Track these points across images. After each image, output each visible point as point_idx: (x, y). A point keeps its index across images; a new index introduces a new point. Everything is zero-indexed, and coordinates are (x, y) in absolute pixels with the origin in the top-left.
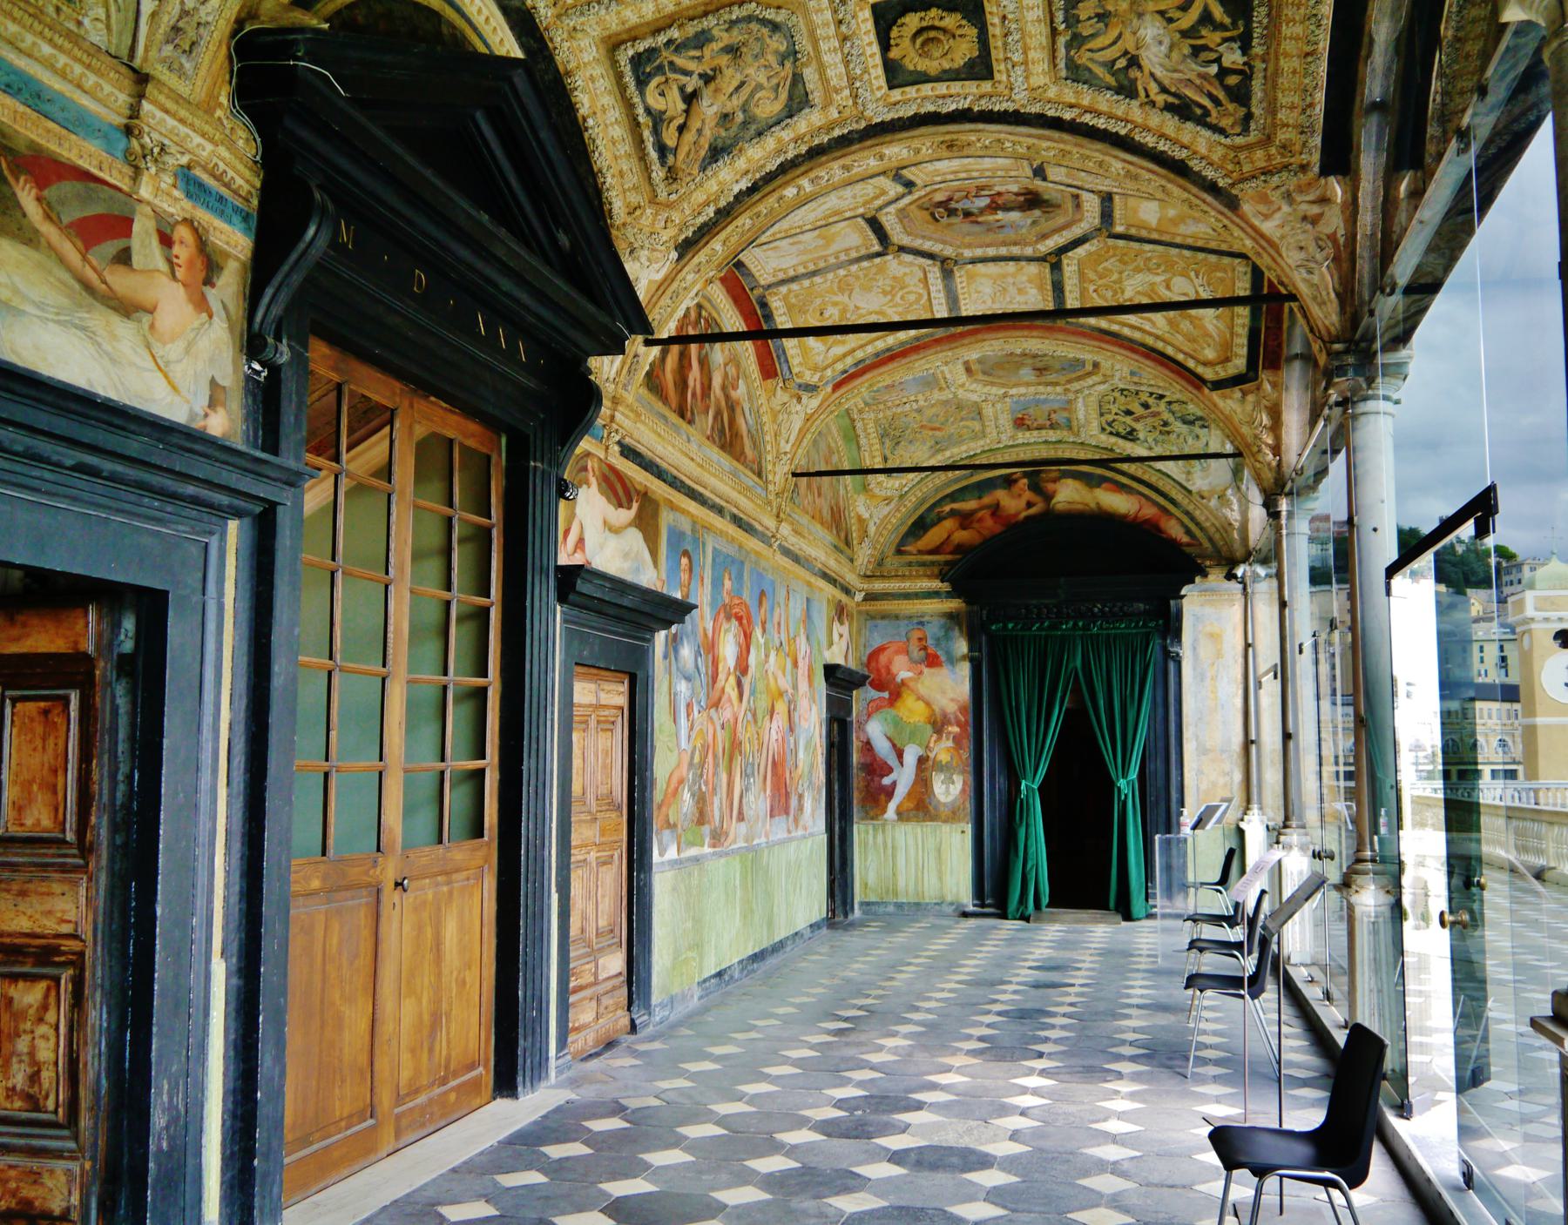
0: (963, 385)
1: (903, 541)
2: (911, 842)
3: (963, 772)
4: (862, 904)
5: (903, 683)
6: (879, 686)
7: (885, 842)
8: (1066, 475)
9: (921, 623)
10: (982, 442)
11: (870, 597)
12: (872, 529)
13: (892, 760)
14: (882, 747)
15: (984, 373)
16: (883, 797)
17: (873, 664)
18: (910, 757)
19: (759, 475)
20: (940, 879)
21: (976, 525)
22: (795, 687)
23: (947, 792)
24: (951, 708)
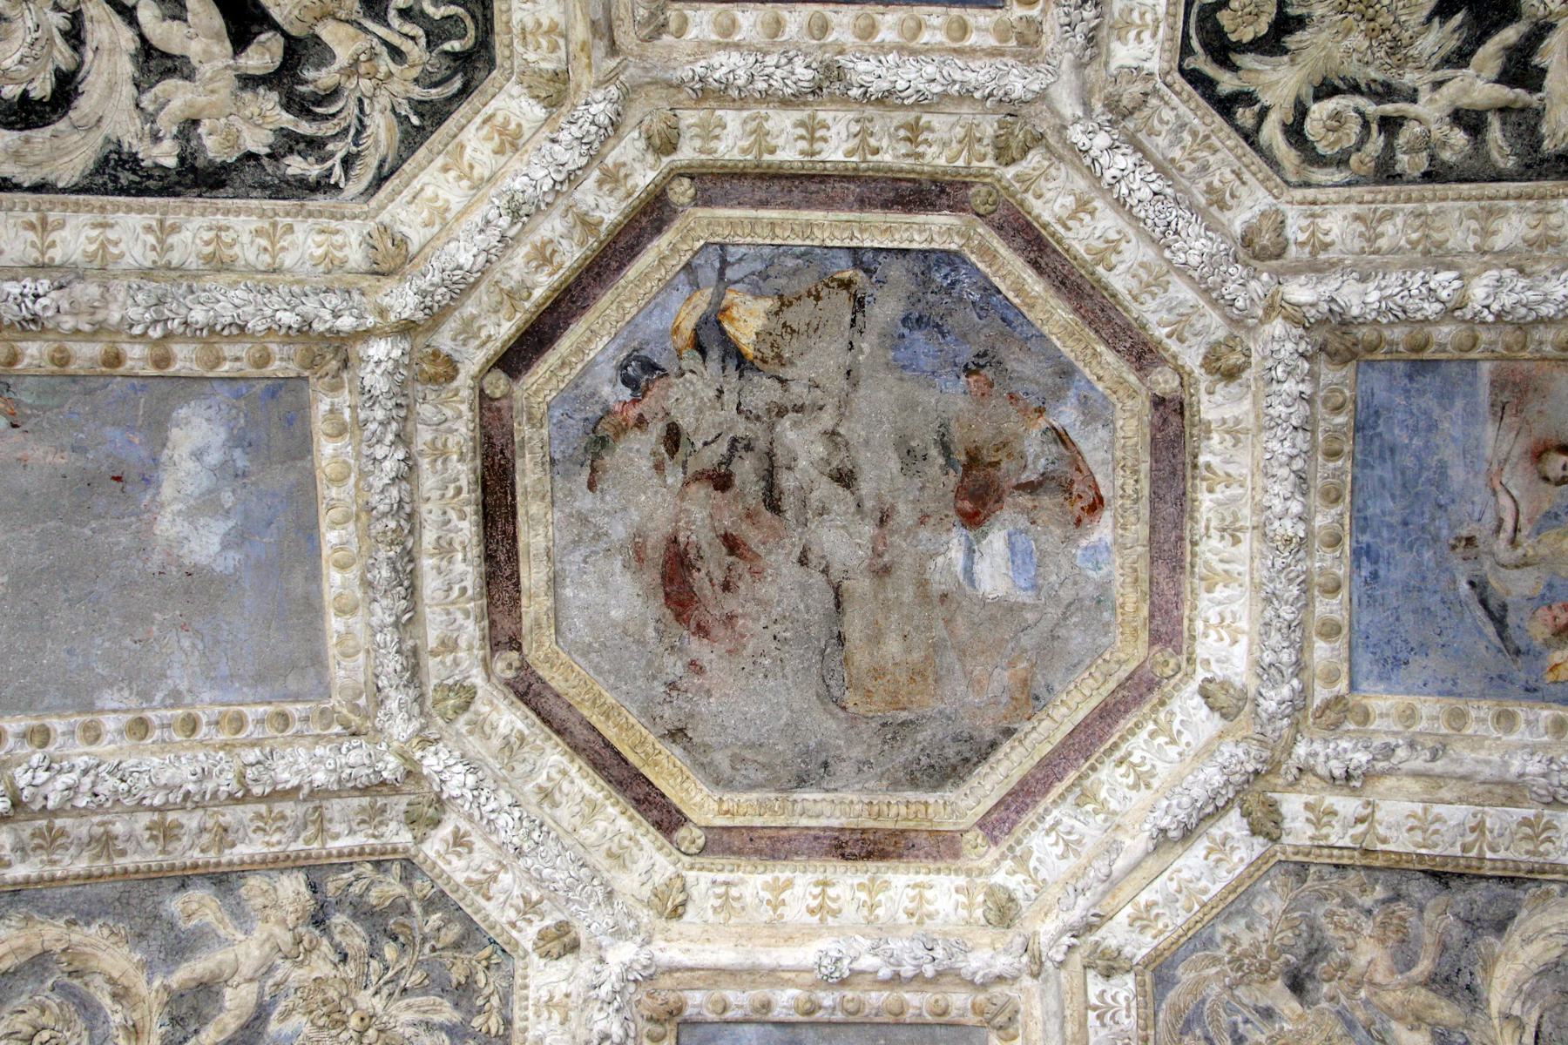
0: (1004, 912)
15: (946, 772)
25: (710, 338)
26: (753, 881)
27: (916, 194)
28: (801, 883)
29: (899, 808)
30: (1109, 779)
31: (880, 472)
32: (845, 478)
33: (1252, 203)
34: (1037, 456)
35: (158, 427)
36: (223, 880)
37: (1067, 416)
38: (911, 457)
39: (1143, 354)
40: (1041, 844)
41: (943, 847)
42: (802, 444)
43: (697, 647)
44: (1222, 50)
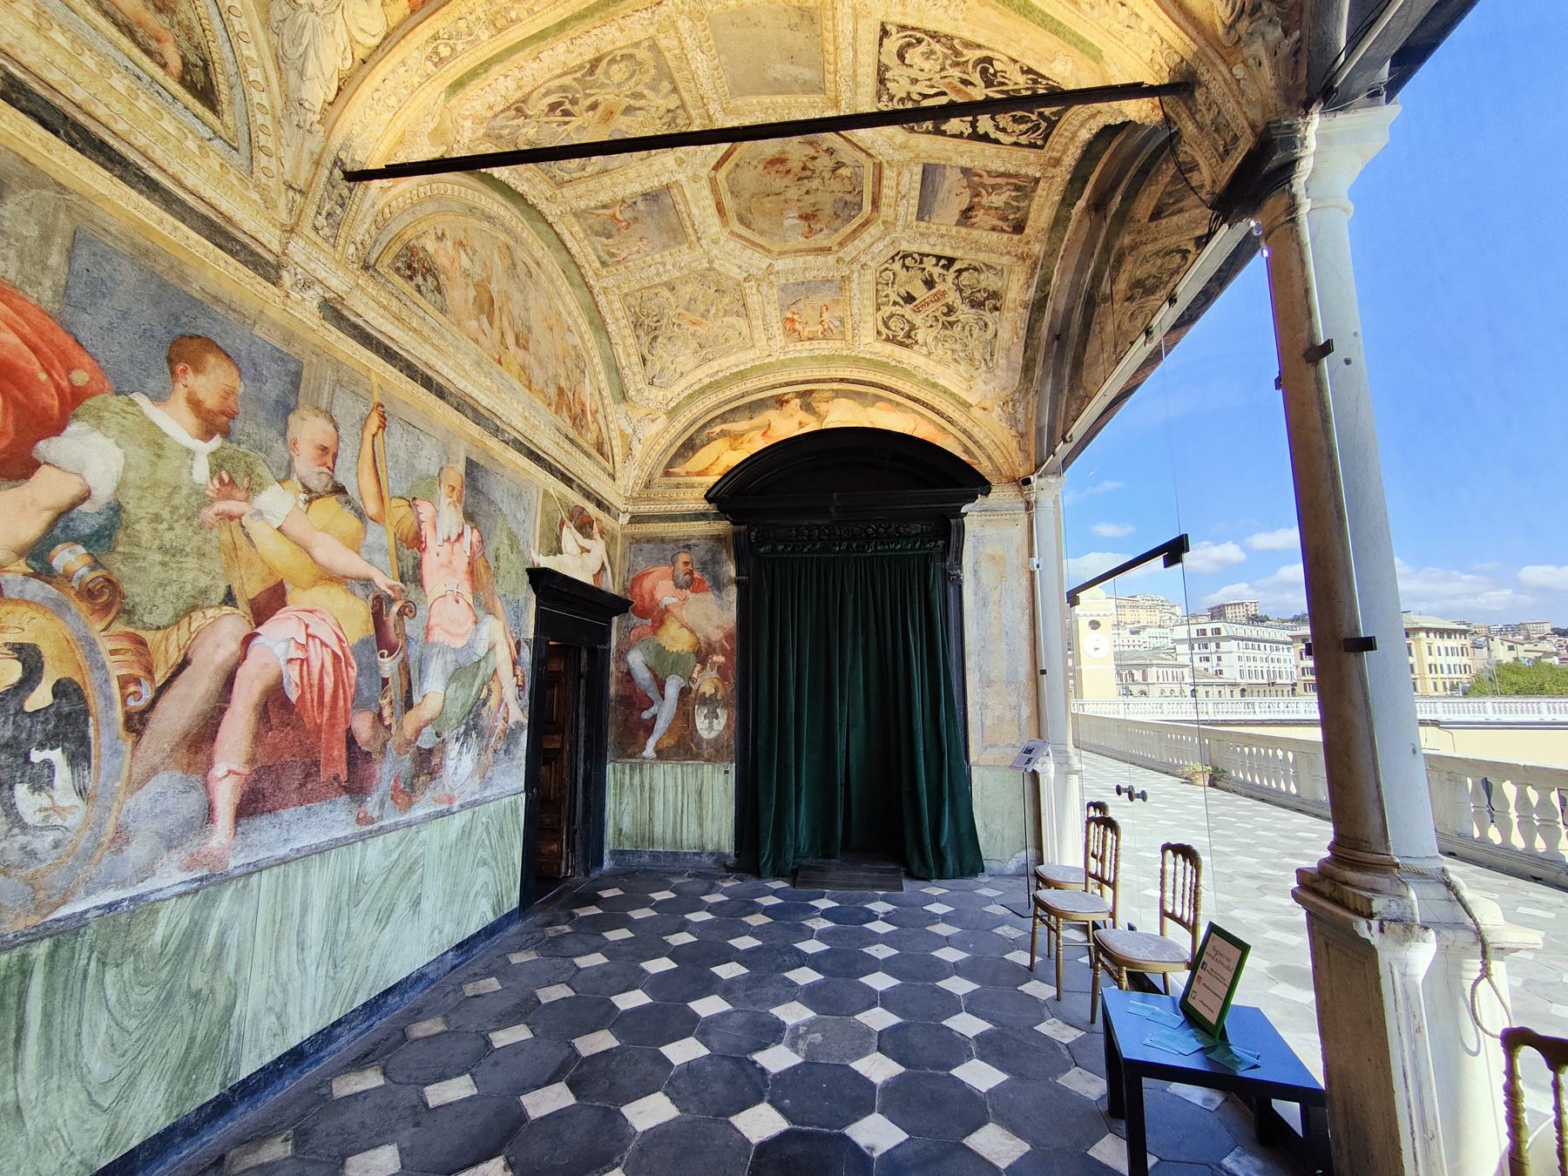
0: (715, 242)
1: (670, 464)
2: (670, 782)
3: (725, 706)
4: (614, 853)
5: (667, 610)
6: (643, 614)
7: (642, 785)
8: (838, 394)
9: (688, 547)
10: (751, 354)
11: (636, 519)
12: (638, 450)
13: (653, 694)
14: (642, 675)
15: (742, 220)
16: (641, 733)
17: (637, 590)
18: (672, 688)
19: (206, 94)
20: (701, 825)
21: (745, 445)
22: (413, 576)
23: (711, 727)
24: (717, 636)
25: (840, 165)
26: (707, 192)
27: (875, 203)
28: (709, 202)
29: (732, 215)
30: (749, 252)
31: (811, 199)
32: (807, 192)
33: (873, 264)
34: (819, 226)
35: (810, 67)
36: (675, 90)
37: (826, 231)
38: (814, 204)
39: (841, 244)
40: (731, 244)
41: (725, 223)
42: (815, 184)
43: (761, 167)
44: (904, 257)
